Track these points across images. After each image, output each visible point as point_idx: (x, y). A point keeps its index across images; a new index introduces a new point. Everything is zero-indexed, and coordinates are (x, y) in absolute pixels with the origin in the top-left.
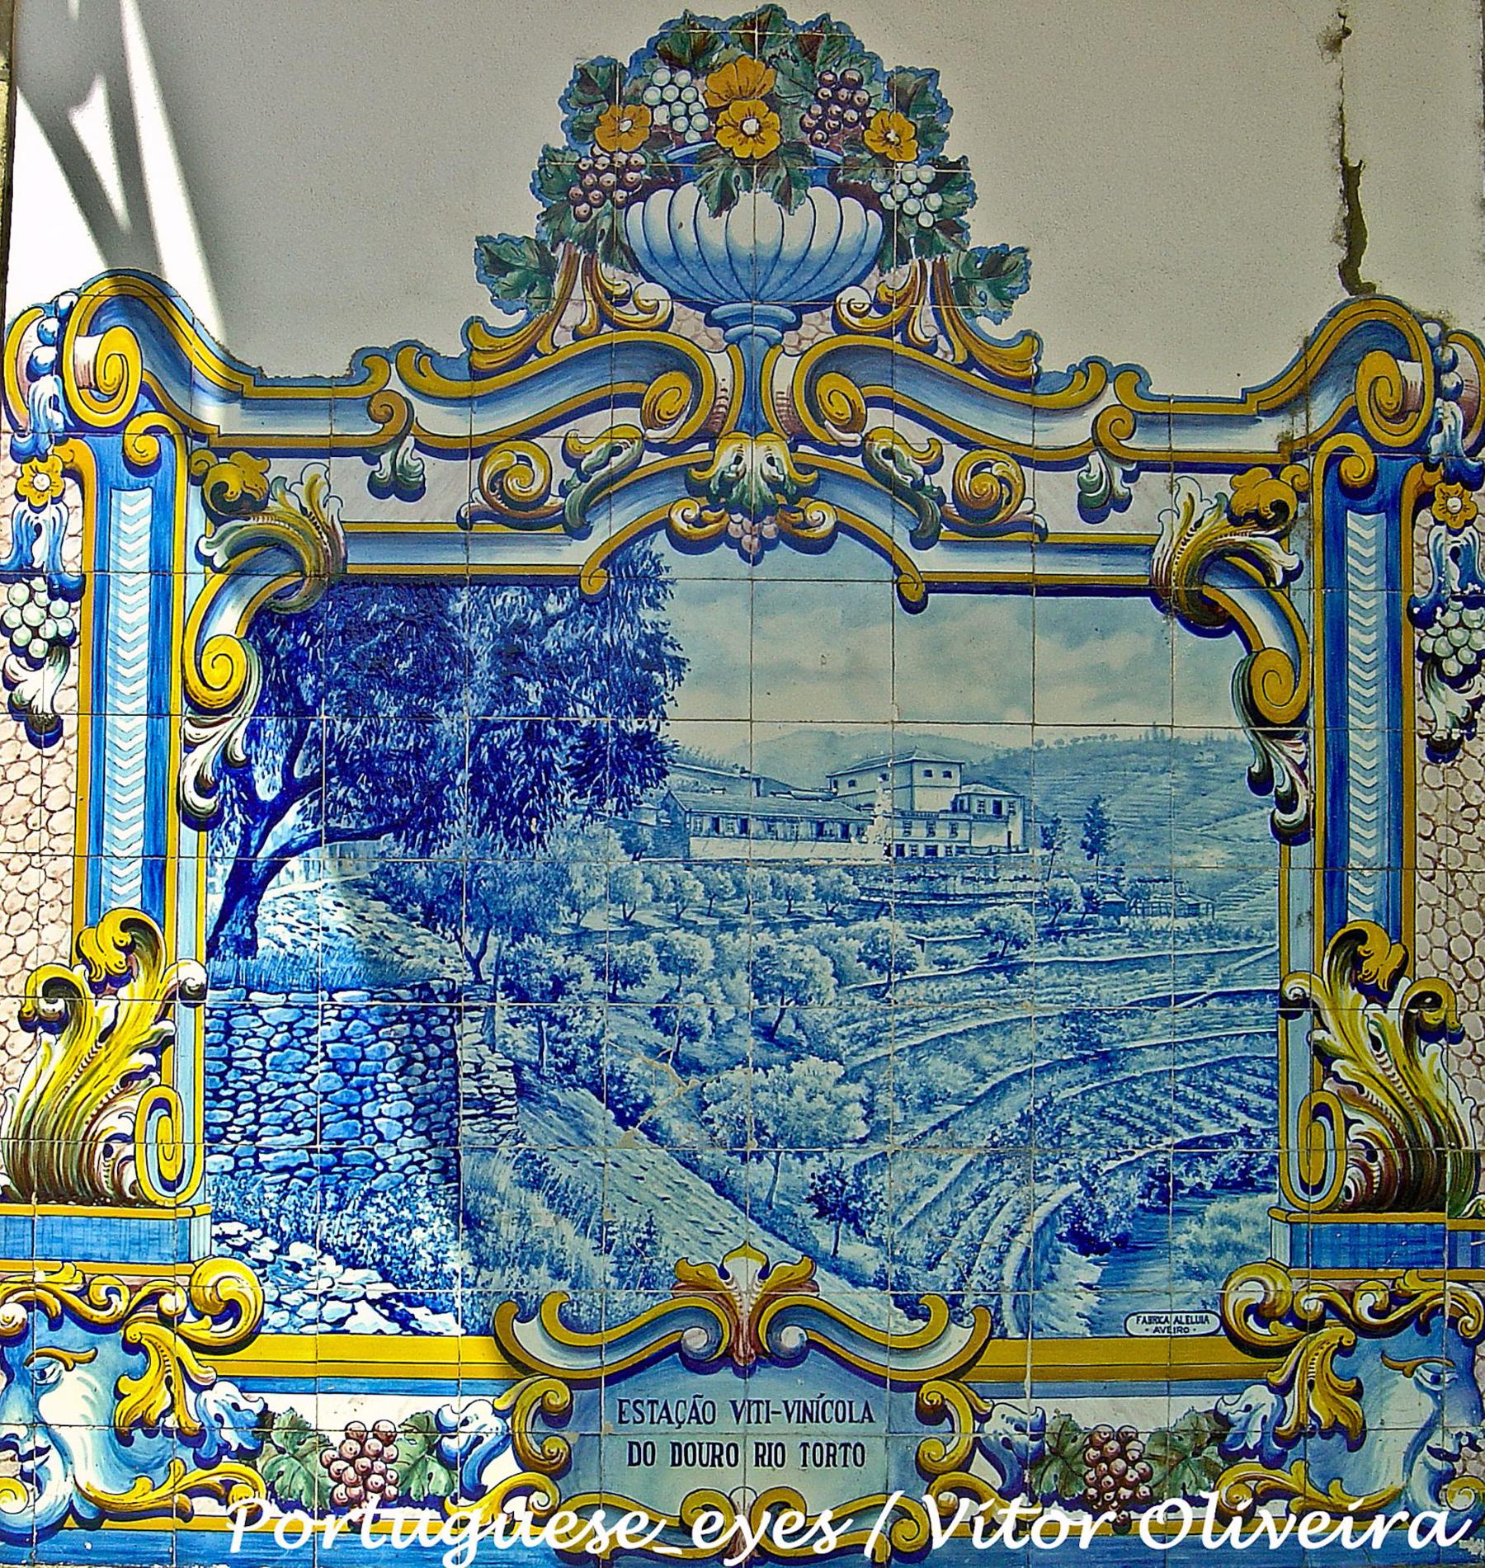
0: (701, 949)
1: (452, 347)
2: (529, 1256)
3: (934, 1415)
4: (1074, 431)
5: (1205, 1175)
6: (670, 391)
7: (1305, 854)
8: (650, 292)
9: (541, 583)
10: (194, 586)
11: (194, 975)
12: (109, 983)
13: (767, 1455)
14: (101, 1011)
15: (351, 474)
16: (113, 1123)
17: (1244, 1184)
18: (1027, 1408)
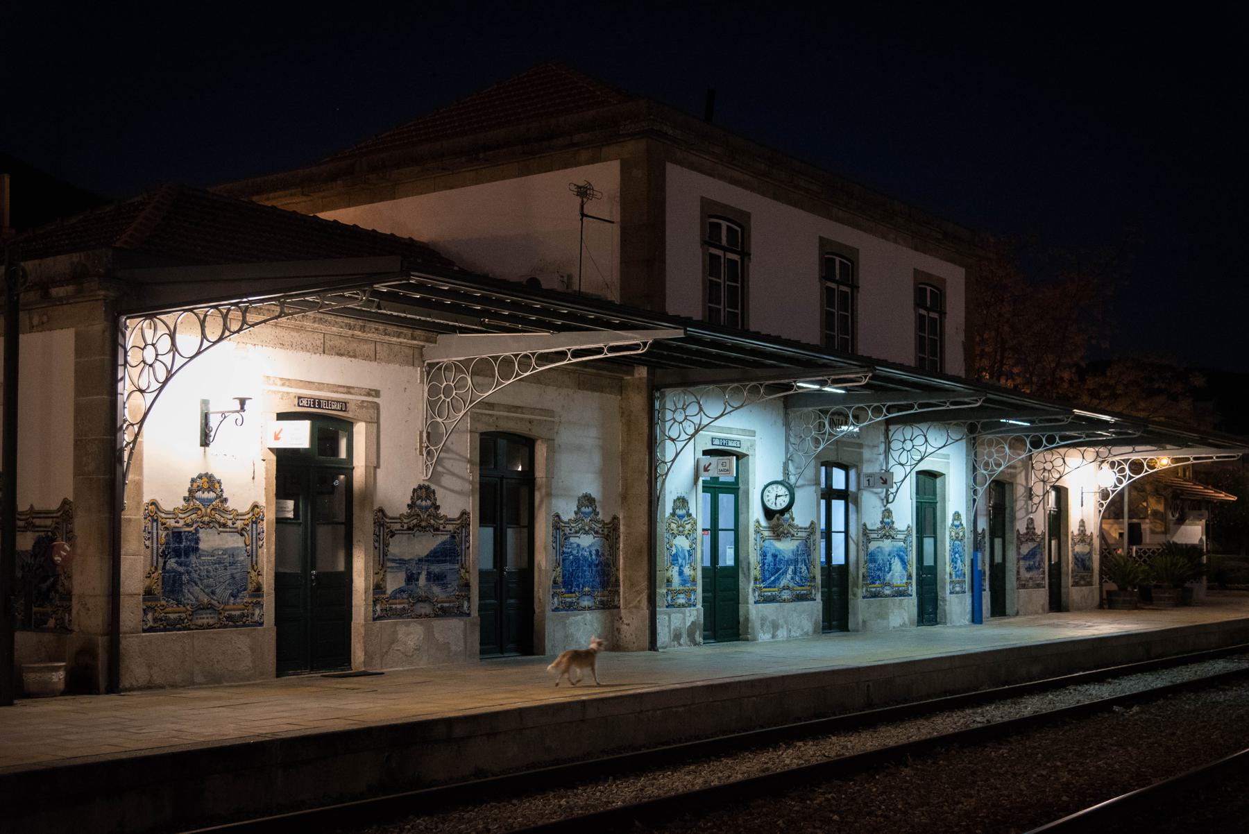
0: (202, 568)
1: (181, 508)
2: (188, 599)
3: (220, 613)
4: (231, 516)
5: (241, 589)
6: (199, 512)
7: (250, 557)
8: (198, 502)
9: (189, 532)
10: (160, 532)
11: (161, 572)
12: (153, 573)
13: (207, 618)
14: (153, 575)
15: (173, 521)
16: (154, 587)
17: (245, 590)
18: (228, 612)
